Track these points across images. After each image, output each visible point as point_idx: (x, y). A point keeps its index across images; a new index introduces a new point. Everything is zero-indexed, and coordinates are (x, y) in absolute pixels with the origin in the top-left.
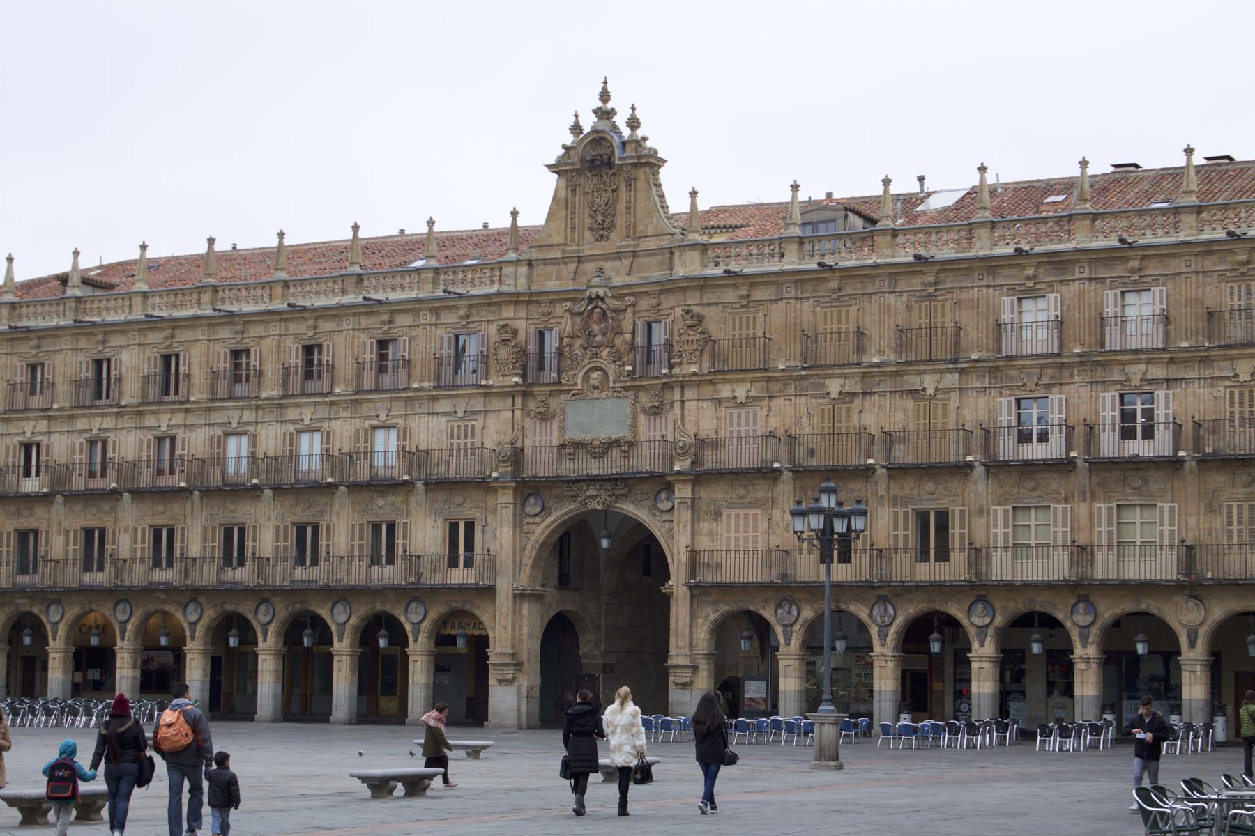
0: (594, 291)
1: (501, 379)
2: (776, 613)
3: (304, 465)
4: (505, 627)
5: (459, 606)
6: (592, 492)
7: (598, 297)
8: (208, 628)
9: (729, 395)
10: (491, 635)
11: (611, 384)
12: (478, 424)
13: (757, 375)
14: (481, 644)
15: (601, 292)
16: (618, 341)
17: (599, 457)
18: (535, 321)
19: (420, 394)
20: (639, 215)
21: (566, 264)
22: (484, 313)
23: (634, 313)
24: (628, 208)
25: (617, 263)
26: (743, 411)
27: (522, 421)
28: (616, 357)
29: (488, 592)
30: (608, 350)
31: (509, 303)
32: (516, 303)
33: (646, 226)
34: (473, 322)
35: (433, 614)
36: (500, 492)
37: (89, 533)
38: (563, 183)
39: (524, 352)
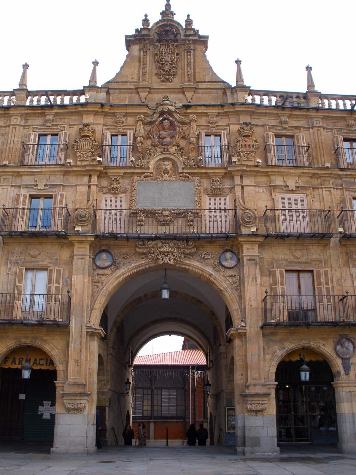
1: (79, 163)
2: (335, 349)
5: (28, 342)
6: (166, 249)
7: (170, 113)
9: (282, 184)
10: (60, 368)
11: (180, 170)
13: (305, 171)
15: (172, 108)
16: (183, 143)
17: (163, 225)
18: (109, 127)
19: (7, 170)
20: (197, 70)
21: (138, 93)
22: (66, 120)
25: (181, 96)
26: (292, 196)
30: (175, 148)
33: (204, 76)
34: (57, 125)
36: (76, 246)
38: (136, 48)
39: (102, 145)
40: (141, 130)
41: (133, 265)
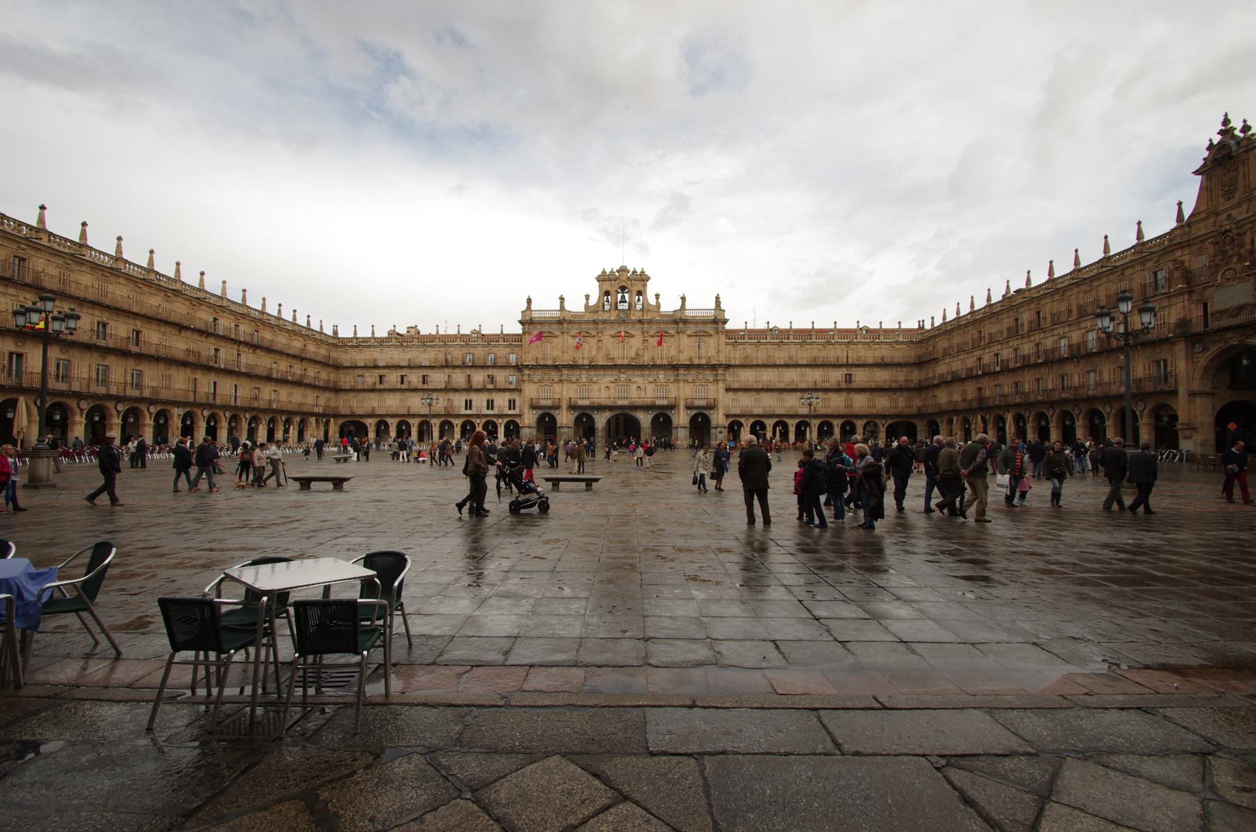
0: (1223, 229)
3: (1090, 345)
4: (1184, 411)
8: (1058, 418)
12: (1166, 313)
14: (1174, 418)
15: (1228, 227)
23: (1252, 233)
24: (1244, 177)
27: (1189, 305)
28: (1241, 258)
29: (1174, 393)
31: (1178, 249)
32: (1182, 248)
35: (1149, 406)
37: (1016, 383)
40: (1212, 251)
41: (1217, 347)
